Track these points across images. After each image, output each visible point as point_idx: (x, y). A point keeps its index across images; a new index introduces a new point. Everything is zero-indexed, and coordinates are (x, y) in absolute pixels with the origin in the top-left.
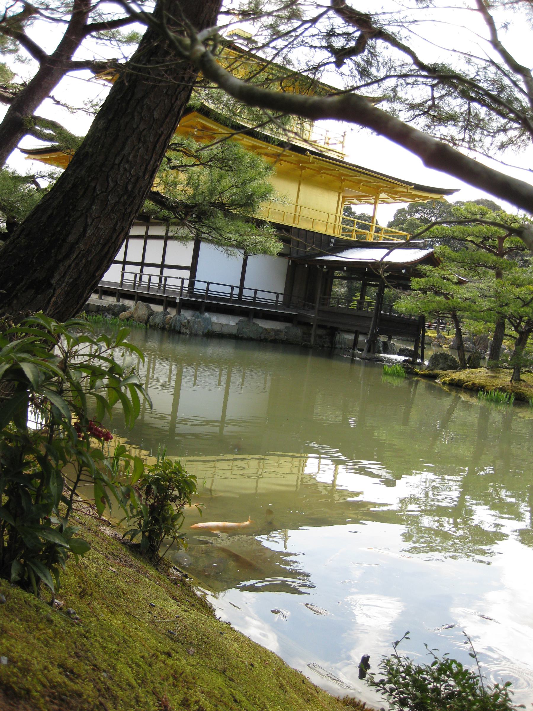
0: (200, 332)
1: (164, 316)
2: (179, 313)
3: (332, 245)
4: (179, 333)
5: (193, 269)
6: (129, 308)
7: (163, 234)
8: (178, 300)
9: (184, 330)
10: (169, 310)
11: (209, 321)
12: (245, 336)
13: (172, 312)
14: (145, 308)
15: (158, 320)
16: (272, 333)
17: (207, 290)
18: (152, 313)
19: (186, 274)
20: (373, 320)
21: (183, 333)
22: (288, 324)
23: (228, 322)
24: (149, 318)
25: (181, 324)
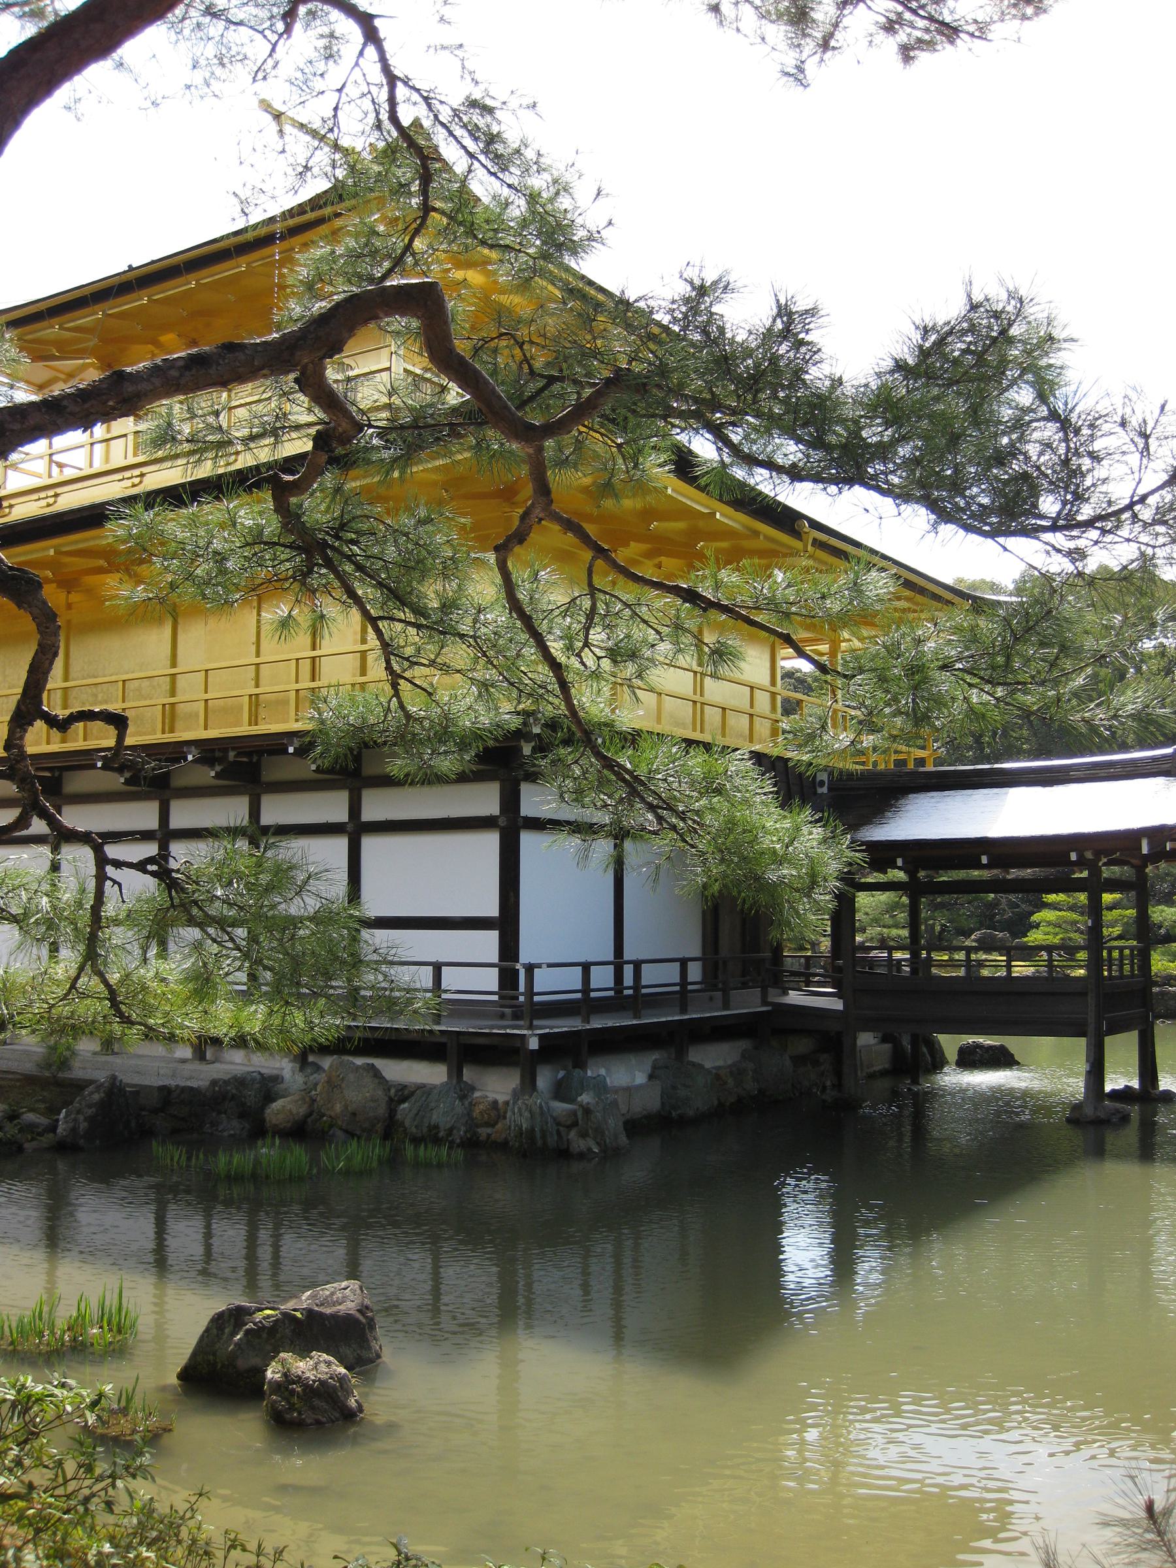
0: (623, 1139)
1: (462, 1098)
2: (529, 1083)
3: (825, 790)
4: (564, 1154)
5: (507, 923)
6: (277, 1079)
7: (340, 815)
8: (534, 1044)
9: (579, 1144)
10: (468, 1074)
11: (600, 1087)
12: (691, 1113)
13: (496, 1086)
14: (368, 1079)
15: (442, 1115)
16: (730, 1081)
17: (586, 988)
18: (404, 1093)
19: (487, 944)
20: (1091, 1000)
21: (581, 1156)
22: (744, 1044)
23: (627, 1077)
24: (392, 1112)
25: (558, 1124)
